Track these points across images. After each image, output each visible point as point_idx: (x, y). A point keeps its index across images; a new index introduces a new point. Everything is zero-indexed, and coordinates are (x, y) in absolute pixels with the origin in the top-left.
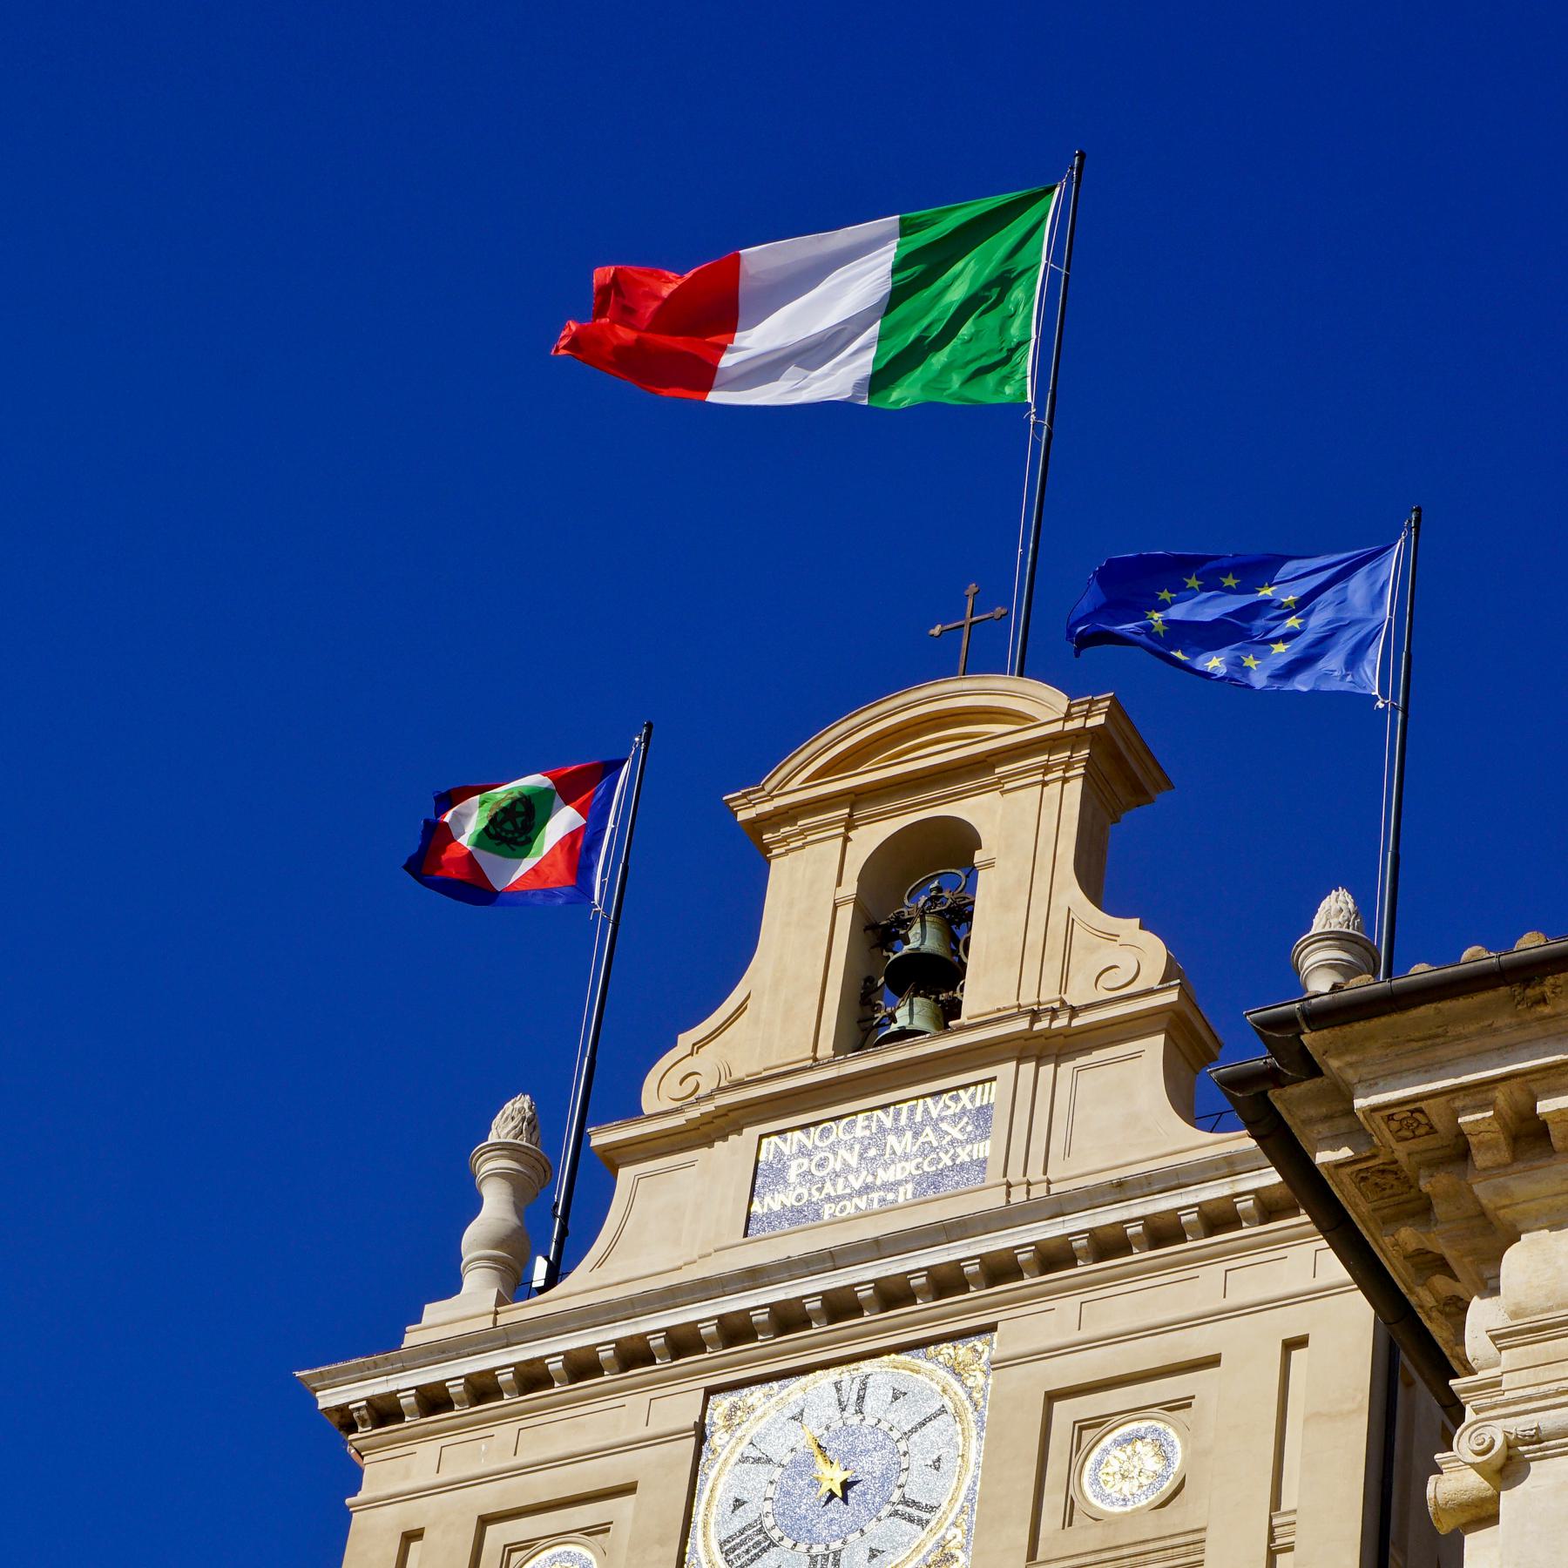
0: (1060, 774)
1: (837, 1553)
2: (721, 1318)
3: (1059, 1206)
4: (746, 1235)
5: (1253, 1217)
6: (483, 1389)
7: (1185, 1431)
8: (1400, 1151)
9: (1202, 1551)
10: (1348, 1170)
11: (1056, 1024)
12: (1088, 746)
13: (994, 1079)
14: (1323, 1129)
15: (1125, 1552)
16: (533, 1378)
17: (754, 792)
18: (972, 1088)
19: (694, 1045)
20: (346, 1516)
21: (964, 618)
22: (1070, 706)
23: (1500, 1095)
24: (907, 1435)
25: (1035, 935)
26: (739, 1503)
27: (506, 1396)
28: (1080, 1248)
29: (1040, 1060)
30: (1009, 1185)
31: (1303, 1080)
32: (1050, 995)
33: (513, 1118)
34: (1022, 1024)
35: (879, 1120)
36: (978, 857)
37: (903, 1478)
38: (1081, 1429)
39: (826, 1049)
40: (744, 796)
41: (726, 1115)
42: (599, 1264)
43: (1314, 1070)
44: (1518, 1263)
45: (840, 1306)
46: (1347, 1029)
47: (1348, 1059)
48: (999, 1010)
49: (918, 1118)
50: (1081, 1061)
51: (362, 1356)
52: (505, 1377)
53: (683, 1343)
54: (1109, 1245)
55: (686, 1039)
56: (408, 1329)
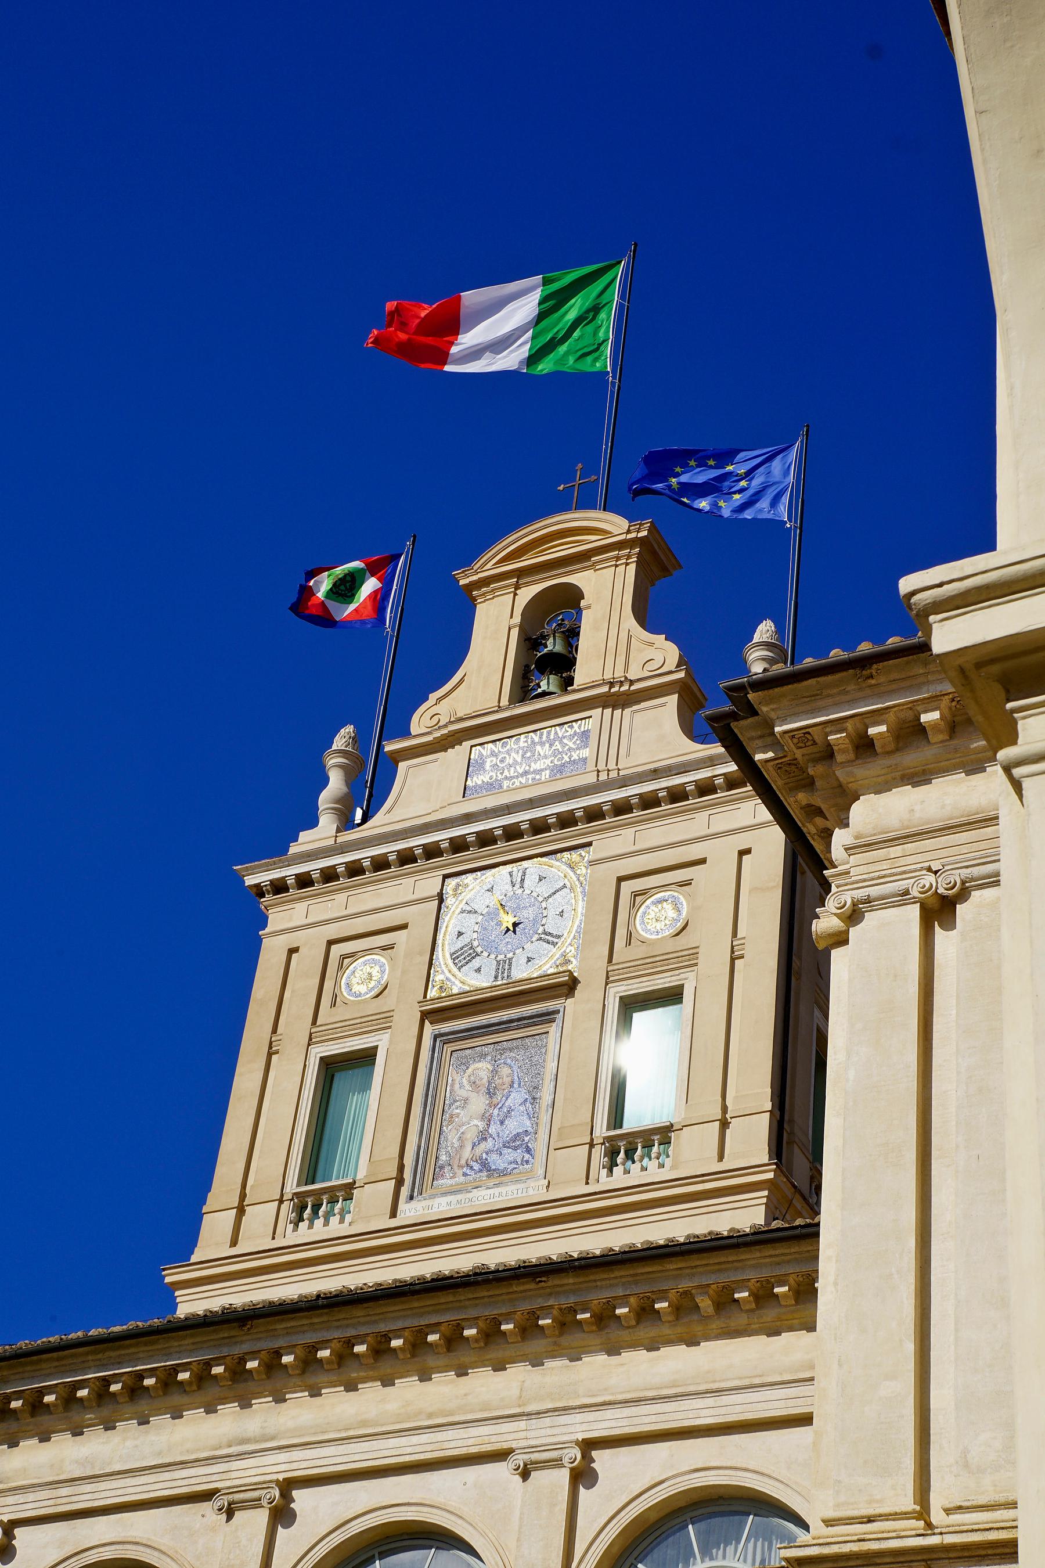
0: (625, 561)
1: (510, 959)
2: (451, 839)
3: (624, 782)
4: (464, 797)
5: (723, 787)
6: (329, 875)
7: (688, 896)
8: (799, 754)
9: (697, 959)
10: (772, 763)
11: (622, 689)
12: (638, 547)
13: (591, 717)
14: (759, 743)
15: (658, 959)
16: (355, 870)
17: (468, 570)
18: (580, 722)
19: (437, 699)
20: (259, 941)
21: (575, 481)
22: (629, 526)
23: (849, 725)
24: (546, 899)
25: (612, 644)
26: (460, 934)
27: (341, 879)
28: (635, 803)
29: (614, 708)
30: (598, 771)
31: (748, 718)
32: (619, 674)
33: (345, 737)
34: (605, 689)
35: (532, 738)
36: (583, 603)
37: (544, 920)
38: (635, 896)
39: (505, 701)
40: (463, 572)
41: (454, 735)
42: (389, 811)
43: (754, 712)
44: (858, 811)
45: (512, 833)
46: (771, 691)
47: (772, 706)
48: (593, 682)
49: (552, 737)
50: (635, 707)
51: (267, 858)
52: (341, 869)
53: (432, 852)
54: (649, 802)
55: (433, 697)
56: (291, 844)
